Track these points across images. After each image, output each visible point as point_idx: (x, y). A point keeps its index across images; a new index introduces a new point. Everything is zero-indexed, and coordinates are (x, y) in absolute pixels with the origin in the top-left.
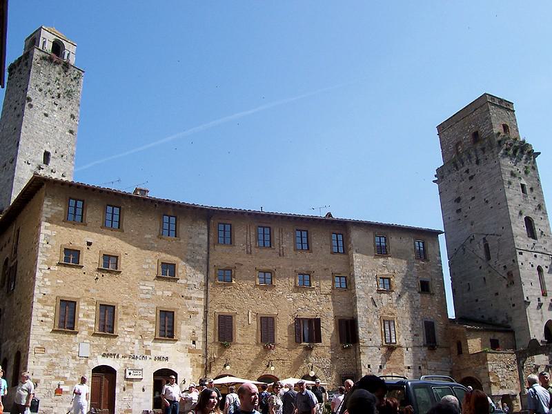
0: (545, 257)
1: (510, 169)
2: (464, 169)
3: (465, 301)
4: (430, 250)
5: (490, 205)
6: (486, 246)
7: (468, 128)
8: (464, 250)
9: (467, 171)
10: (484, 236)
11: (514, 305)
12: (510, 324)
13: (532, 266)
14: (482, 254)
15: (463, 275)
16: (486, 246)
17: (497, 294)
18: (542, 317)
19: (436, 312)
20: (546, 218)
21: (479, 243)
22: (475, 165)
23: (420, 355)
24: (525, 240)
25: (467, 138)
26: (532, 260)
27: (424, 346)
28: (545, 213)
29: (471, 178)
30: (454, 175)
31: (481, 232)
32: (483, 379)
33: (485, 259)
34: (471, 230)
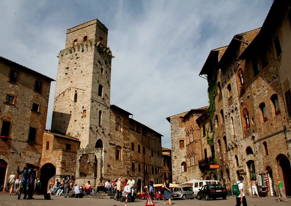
0: (104, 107)
1: (98, 59)
2: (75, 53)
3: (58, 122)
4: (44, 87)
5: (83, 74)
6: (76, 95)
7: (83, 34)
8: (64, 95)
9: (76, 55)
10: (76, 89)
11: (83, 128)
12: (78, 138)
13: (97, 110)
14: (73, 98)
15: (60, 108)
16: (76, 95)
17: (76, 121)
18: (96, 137)
19: (39, 123)
20: (110, 88)
21: (72, 92)
22: (81, 53)
23: (22, 146)
24: (96, 96)
25: (81, 39)
26: (97, 107)
27: (27, 142)
28: (109, 86)
29: (77, 58)
30: (69, 55)
31: (75, 87)
32: (57, 165)
33: (73, 101)
34: (70, 85)
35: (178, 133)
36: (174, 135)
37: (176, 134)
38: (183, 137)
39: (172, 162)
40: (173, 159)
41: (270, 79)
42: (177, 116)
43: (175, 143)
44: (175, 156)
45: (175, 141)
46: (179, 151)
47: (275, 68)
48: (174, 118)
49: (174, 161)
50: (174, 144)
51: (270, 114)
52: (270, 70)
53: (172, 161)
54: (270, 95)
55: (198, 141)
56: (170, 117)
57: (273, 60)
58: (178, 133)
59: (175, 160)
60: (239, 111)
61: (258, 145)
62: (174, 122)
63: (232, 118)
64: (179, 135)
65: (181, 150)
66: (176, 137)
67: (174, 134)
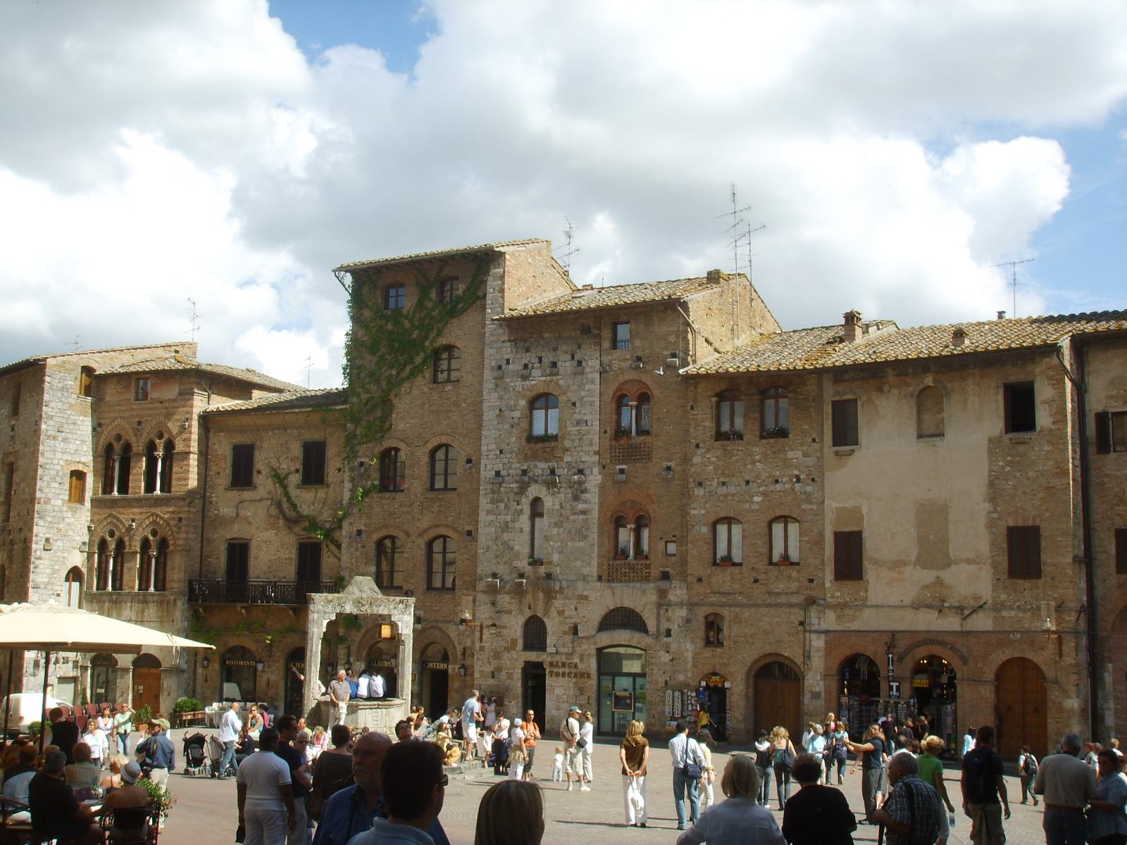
35: (69, 436)
36: (52, 443)
37: (60, 439)
38: (83, 459)
39: (32, 566)
40: (35, 552)
41: (783, 476)
42: (75, 359)
43: (53, 479)
44: (47, 540)
45: (53, 473)
46: (63, 519)
47: (811, 461)
48: (61, 366)
49: (40, 558)
50: (48, 483)
51: (757, 554)
52: (790, 455)
53: (32, 560)
54: (771, 512)
55: (197, 501)
56: (45, 359)
57: (810, 440)
58: (69, 436)
59: (46, 555)
60: (593, 498)
61: (684, 614)
62: (59, 385)
63: (536, 502)
64: (72, 447)
65: (69, 514)
66: (59, 455)
67: (55, 438)
